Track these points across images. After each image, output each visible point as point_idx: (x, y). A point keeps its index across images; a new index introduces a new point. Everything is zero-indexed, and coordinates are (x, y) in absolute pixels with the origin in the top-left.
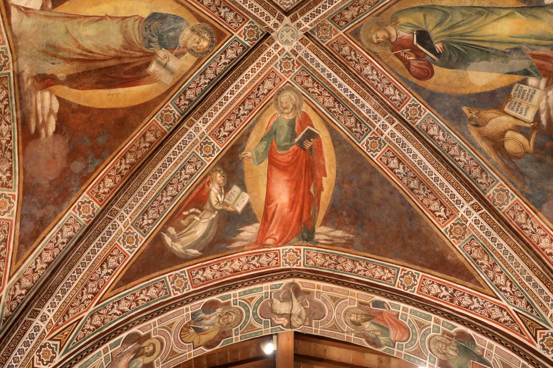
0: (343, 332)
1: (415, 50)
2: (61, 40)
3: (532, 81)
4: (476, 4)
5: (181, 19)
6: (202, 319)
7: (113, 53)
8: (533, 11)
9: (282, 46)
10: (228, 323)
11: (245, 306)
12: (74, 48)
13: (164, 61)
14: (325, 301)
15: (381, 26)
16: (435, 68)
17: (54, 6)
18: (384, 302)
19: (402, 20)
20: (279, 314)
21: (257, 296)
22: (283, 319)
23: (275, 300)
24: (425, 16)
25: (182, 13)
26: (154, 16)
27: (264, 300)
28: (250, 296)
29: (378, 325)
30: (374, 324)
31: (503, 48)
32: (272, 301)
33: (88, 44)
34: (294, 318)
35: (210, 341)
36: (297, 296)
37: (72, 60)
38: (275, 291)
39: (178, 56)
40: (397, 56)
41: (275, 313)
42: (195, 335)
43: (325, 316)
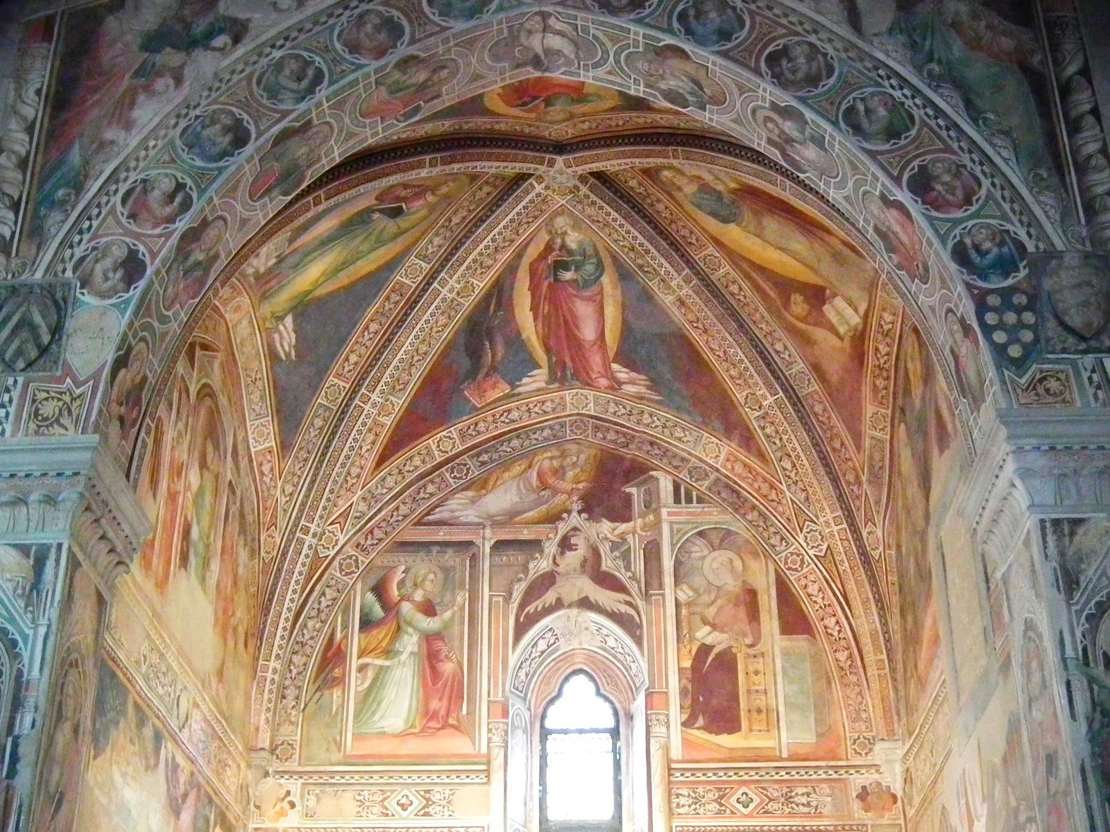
0: (456, 45)
1: (405, 199)
2: (827, 258)
3: (273, 261)
4: (351, 268)
5: (693, 204)
6: (690, 93)
7: (776, 217)
8: (298, 301)
9: (569, 170)
10: (650, 62)
11: (621, 69)
12: (816, 245)
13: (717, 182)
14: (491, 68)
15: (446, 196)
16: (375, 202)
17: (823, 289)
18: (404, 121)
19: (423, 212)
20: (563, 36)
21: (600, 72)
22: (557, 28)
23: (572, 57)
24: (399, 227)
25: (691, 209)
26: (726, 221)
27: (590, 63)
28: (612, 78)
29: (408, 87)
30: (413, 85)
31: (309, 258)
32: (577, 56)
33: (802, 239)
34: (539, 27)
35: (681, 58)
36: (537, 57)
37: (822, 239)
38: (573, 69)
39: (699, 178)
40: (421, 186)
41: (570, 39)
42: (704, 83)
43: (490, 50)
